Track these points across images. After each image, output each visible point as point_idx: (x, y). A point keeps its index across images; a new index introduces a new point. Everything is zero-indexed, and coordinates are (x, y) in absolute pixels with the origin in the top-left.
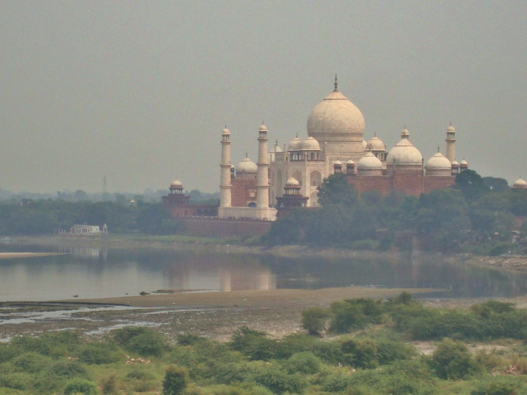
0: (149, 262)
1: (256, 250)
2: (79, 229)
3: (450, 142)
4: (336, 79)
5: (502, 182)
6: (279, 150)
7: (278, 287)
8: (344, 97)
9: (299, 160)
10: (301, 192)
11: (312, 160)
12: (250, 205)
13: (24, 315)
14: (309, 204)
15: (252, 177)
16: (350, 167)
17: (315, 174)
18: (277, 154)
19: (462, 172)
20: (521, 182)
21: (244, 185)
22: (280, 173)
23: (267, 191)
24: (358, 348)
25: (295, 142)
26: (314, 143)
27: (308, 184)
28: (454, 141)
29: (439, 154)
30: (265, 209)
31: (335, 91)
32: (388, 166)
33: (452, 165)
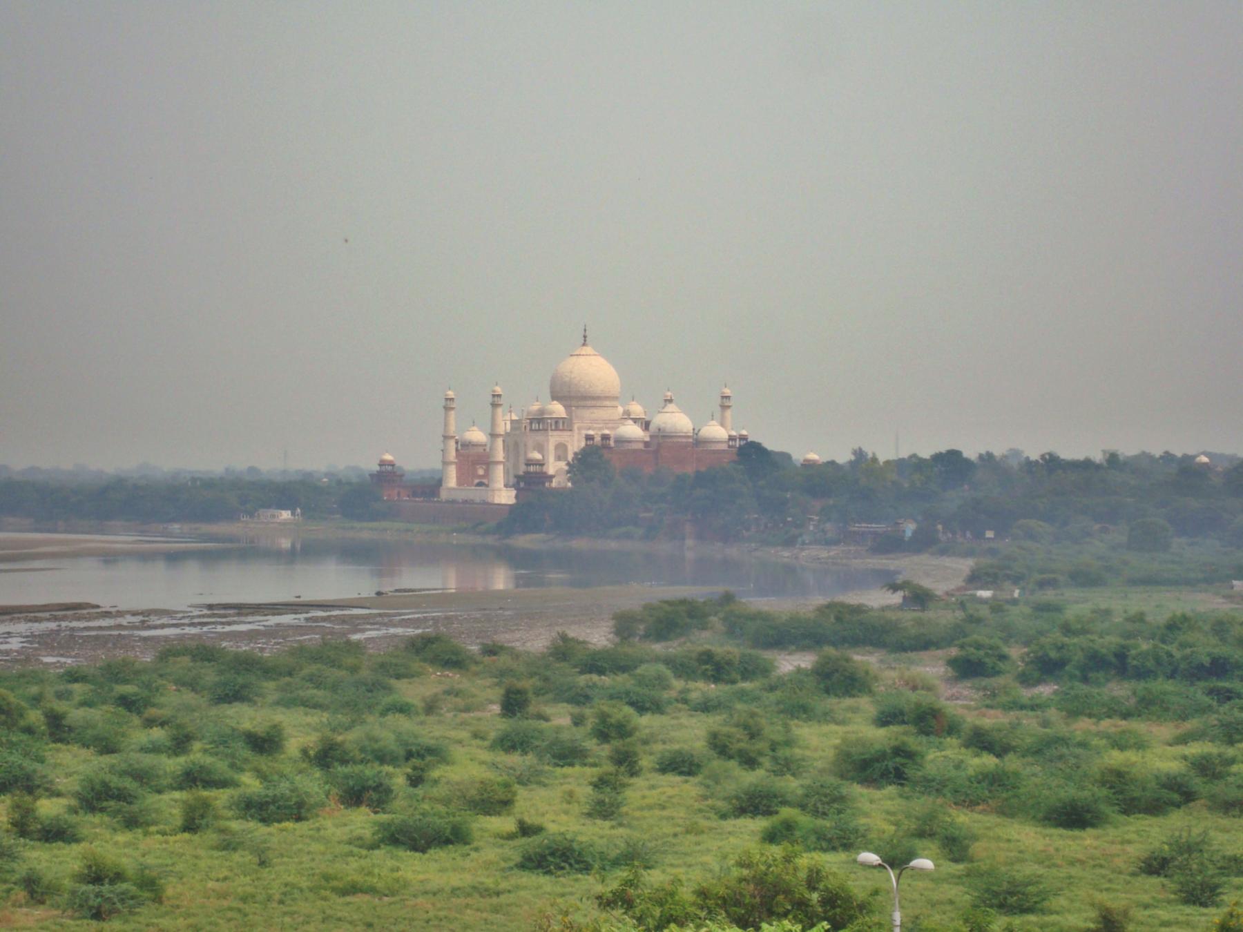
0: (353, 553)
1: (490, 540)
2: (266, 514)
3: (724, 407)
5: (787, 456)
6: (514, 417)
7: (517, 586)
10: (545, 469)
11: (557, 429)
12: (480, 484)
13: (159, 622)
14: (554, 484)
15: (481, 450)
16: (605, 438)
17: (561, 449)
18: (512, 421)
19: (741, 448)
20: (813, 456)
21: (473, 461)
22: (516, 444)
23: (501, 467)
24: (717, 658)
25: (535, 407)
26: (558, 409)
27: (551, 459)
28: (729, 407)
29: (714, 422)
30: (500, 490)
31: (584, 345)
32: (651, 437)
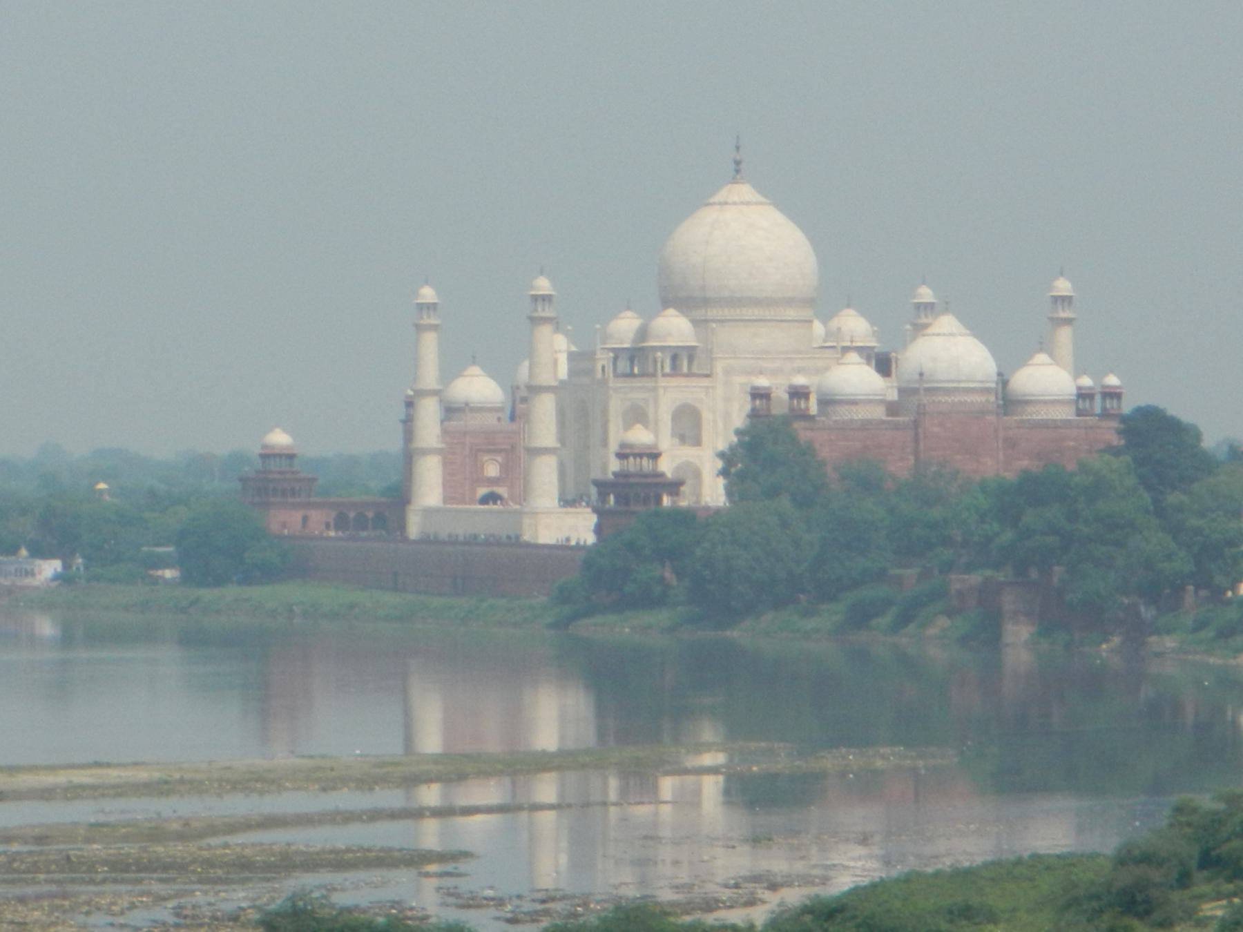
4: (738, 148)
8: (764, 200)
9: (632, 375)
11: (675, 371)
33: (1079, 388)
